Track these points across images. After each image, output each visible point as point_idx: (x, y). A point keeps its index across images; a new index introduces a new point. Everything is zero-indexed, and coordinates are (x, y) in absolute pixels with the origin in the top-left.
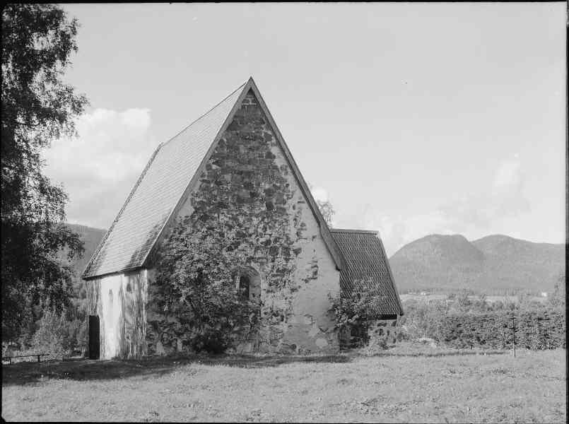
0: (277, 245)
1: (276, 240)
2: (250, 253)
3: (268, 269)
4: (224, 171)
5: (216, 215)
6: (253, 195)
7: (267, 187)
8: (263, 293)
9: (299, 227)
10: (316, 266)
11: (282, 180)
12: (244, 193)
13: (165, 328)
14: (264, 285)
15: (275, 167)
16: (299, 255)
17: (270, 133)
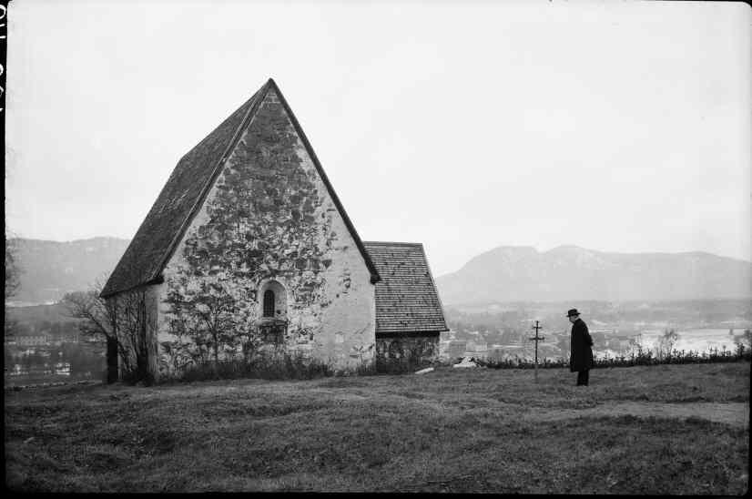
0: (305, 256)
1: (304, 251)
2: (274, 265)
3: (295, 284)
4: (244, 177)
5: (236, 225)
6: (279, 203)
7: (293, 193)
8: (289, 308)
9: (329, 237)
10: (349, 279)
11: (311, 187)
12: (267, 200)
13: (178, 349)
14: (290, 301)
15: (302, 172)
16: (330, 268)
17: (295, 134)
